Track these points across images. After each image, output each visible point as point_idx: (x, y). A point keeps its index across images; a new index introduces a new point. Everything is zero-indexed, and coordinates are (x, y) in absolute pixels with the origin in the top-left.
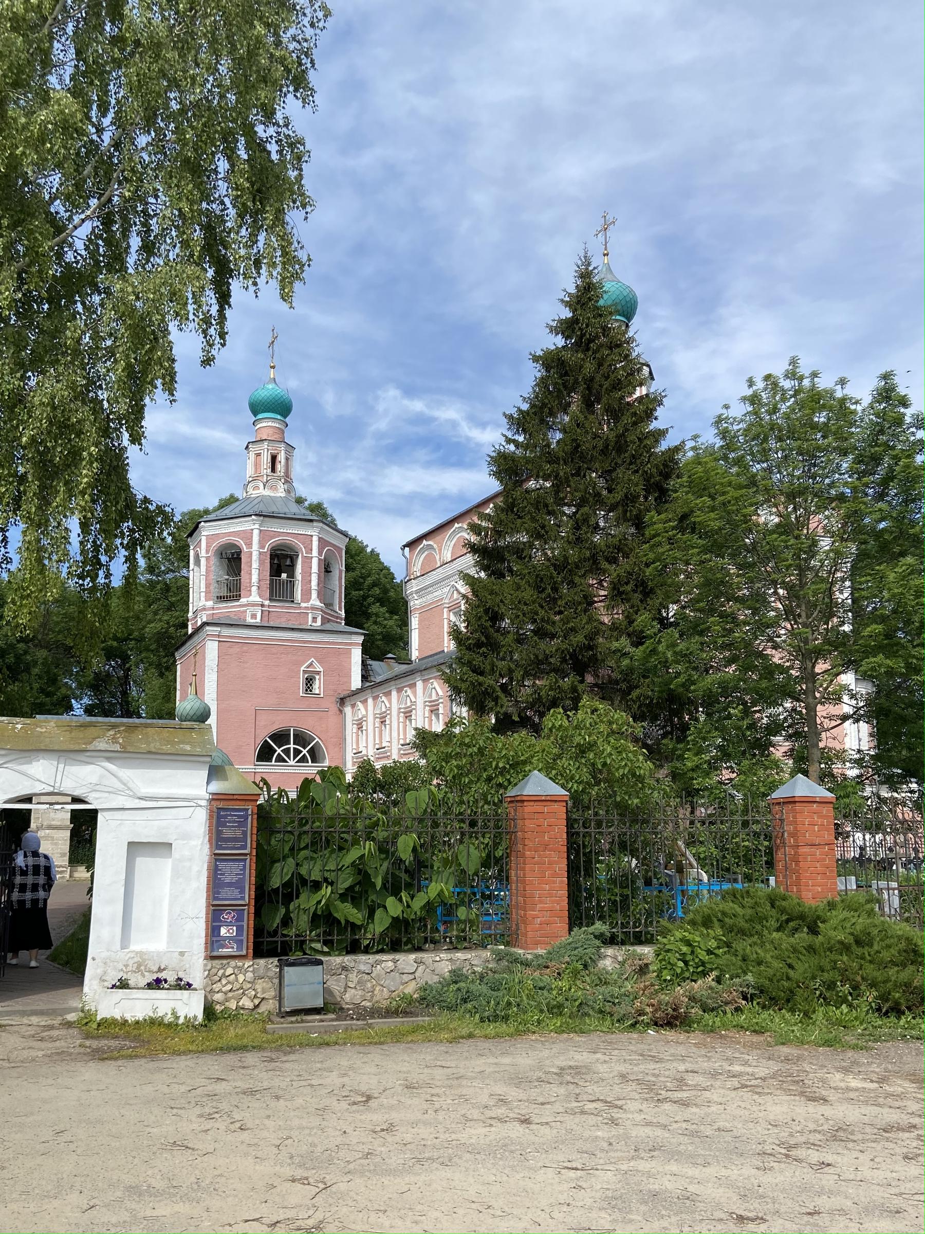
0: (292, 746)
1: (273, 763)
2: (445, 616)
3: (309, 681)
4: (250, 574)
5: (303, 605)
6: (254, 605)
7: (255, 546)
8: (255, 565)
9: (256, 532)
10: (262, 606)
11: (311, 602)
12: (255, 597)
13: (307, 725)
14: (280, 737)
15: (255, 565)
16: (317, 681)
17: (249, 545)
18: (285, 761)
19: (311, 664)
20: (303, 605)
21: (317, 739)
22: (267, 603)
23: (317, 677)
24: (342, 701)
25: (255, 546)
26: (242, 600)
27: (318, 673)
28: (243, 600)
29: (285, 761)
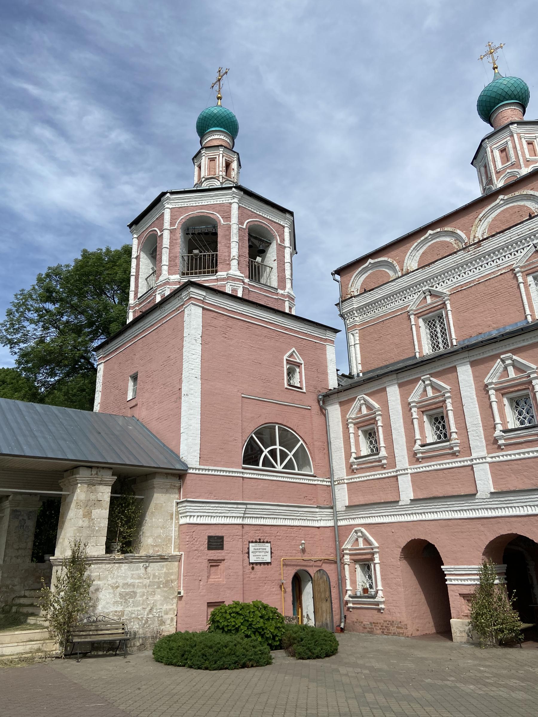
0: (278, 447)
1: (260, 467)
2: (413, 323)
3: (291, 373)
4: (229, 247)
5: (280, 292)
6: (234, 279)
7: (234, 219)
8: (235, 238)
9: (235, 207)
10: (243, 282)
11: (287, 290)
12: (234, 270)
13: (293, 421)
14: (265, 434)
15: (235, 238)
16: (297, 375)
17: (228, 218)
18: (274, 467)
19: (291, 355)
20: (280, 292)
21: (301, 442)
22: (247, 280)
23: (298, 370)
24: (327, 397)
25: (234, 219)
26: (218, 273)
27: (299, 365)
28: (221, 274)
29: (274, 467)
